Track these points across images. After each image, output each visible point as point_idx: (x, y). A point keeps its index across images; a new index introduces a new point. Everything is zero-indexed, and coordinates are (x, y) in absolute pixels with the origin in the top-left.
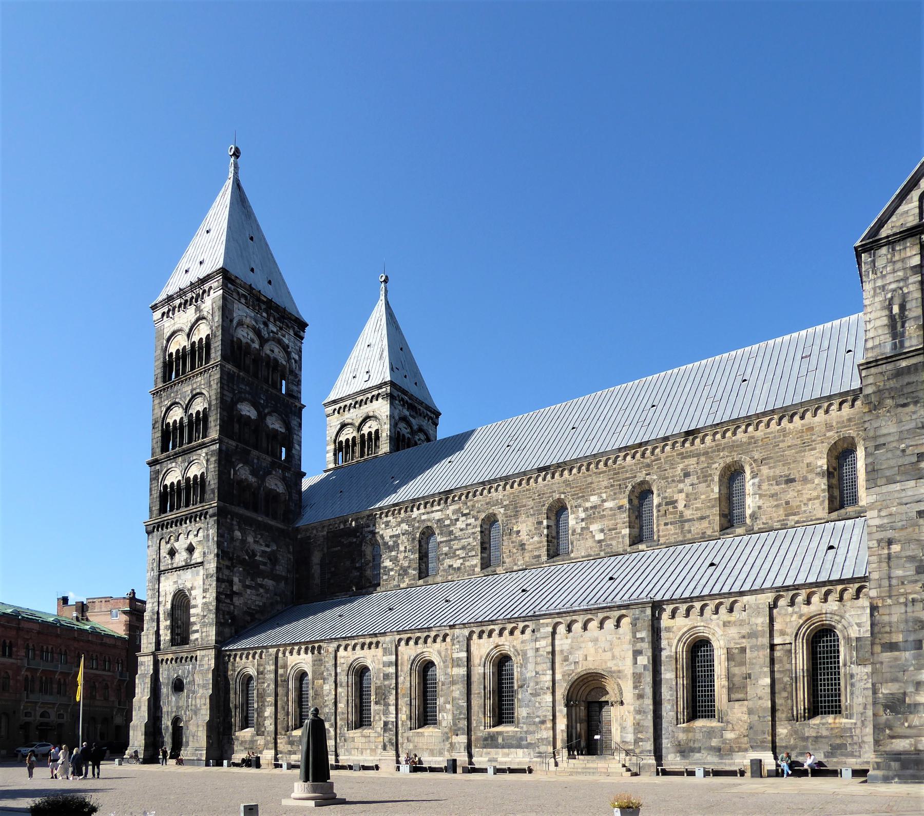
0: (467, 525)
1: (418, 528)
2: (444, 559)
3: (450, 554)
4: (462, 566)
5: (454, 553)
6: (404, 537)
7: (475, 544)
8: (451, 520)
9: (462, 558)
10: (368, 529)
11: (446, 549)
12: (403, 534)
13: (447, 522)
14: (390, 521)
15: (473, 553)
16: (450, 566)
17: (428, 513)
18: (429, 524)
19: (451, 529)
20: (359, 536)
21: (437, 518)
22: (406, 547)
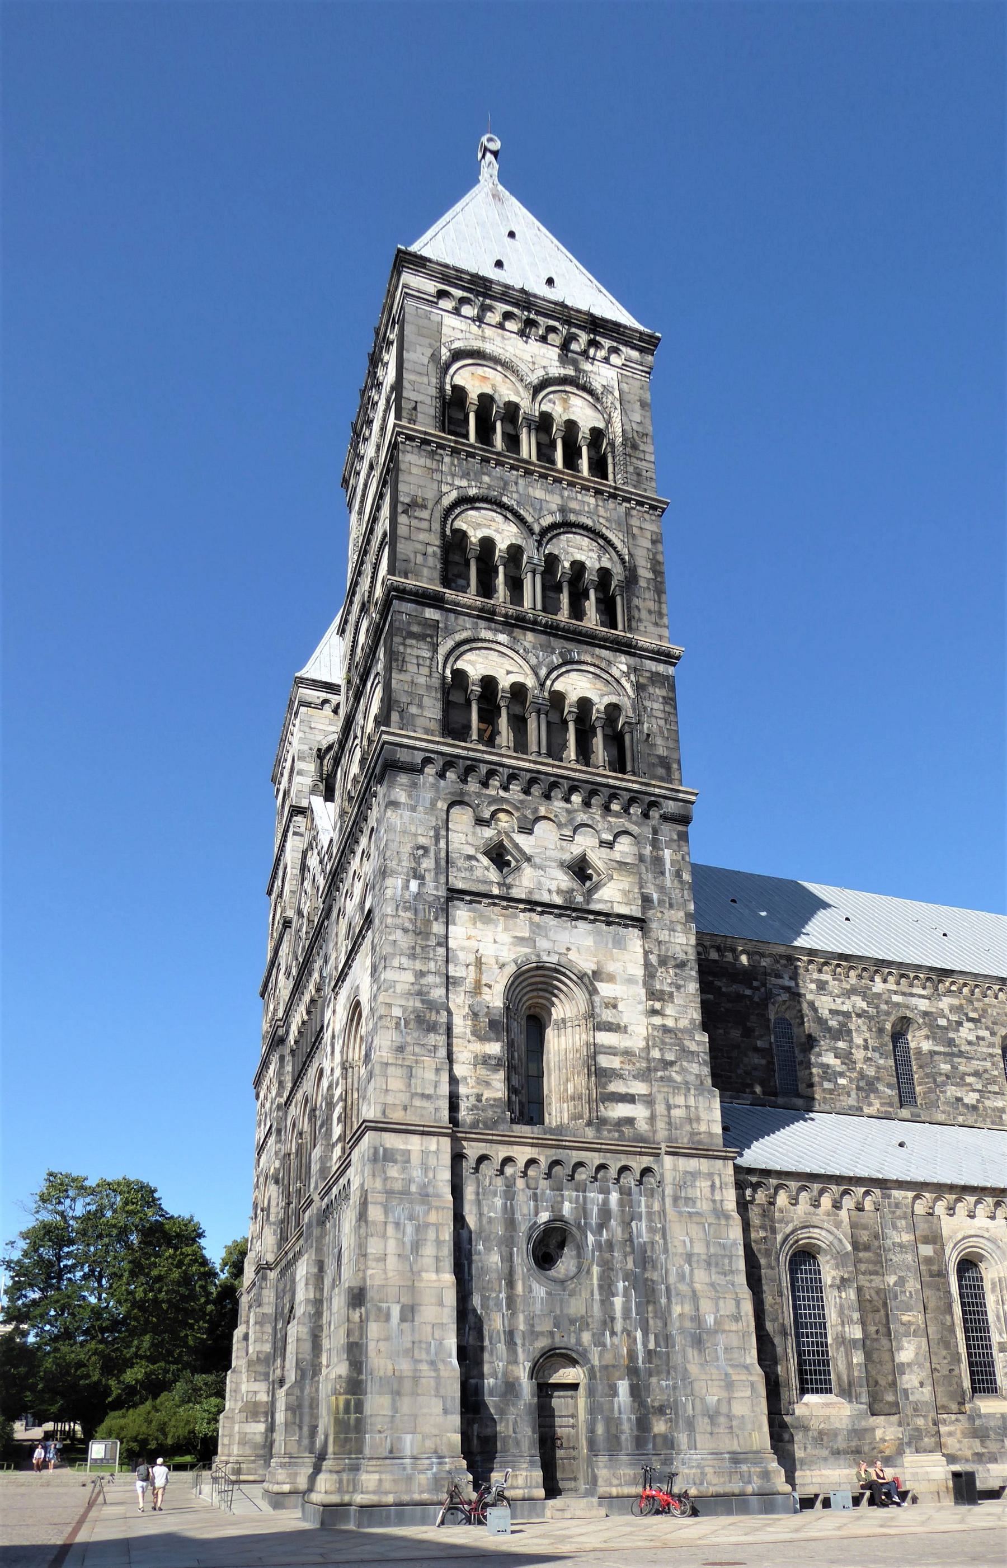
0: (978, 1037)
1: (888, 1014)
2: (944, 1084)
3: (954, 1077)
4: (980, 1105)
5: (962, 1079)
6: (860, 1021)
7: (996, 1073)
8: (948, 1020)
9: (979, 1091)
10: (780, 981)
11: (945, 1067)
12: (859, 1016)
13: (942, 1022)
14: (827, 982)
15: (996, 1089)
16: (959, 1099)
17: (904, 994)
18: (909, 1014)
19: (951, 1035)
20: (757, 989)
21: (923, 1008)
22: (866, 1040)
